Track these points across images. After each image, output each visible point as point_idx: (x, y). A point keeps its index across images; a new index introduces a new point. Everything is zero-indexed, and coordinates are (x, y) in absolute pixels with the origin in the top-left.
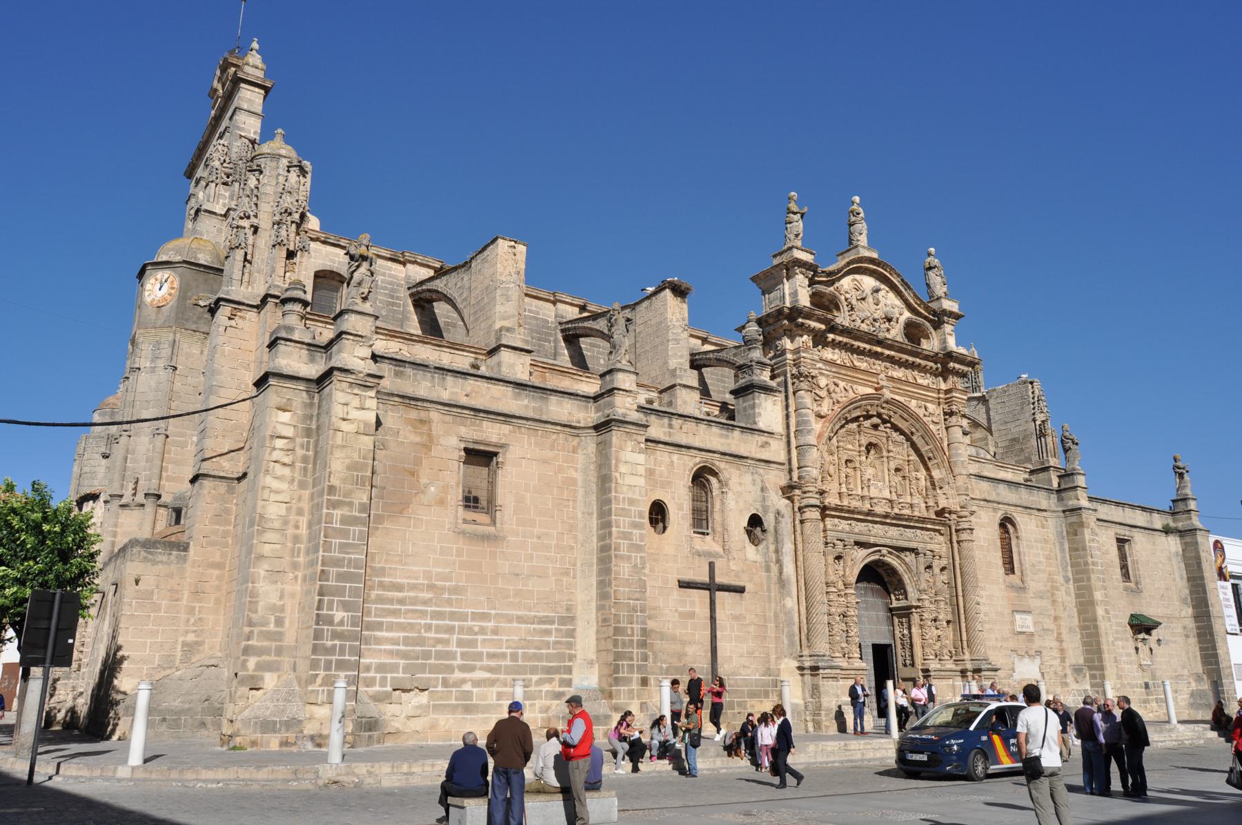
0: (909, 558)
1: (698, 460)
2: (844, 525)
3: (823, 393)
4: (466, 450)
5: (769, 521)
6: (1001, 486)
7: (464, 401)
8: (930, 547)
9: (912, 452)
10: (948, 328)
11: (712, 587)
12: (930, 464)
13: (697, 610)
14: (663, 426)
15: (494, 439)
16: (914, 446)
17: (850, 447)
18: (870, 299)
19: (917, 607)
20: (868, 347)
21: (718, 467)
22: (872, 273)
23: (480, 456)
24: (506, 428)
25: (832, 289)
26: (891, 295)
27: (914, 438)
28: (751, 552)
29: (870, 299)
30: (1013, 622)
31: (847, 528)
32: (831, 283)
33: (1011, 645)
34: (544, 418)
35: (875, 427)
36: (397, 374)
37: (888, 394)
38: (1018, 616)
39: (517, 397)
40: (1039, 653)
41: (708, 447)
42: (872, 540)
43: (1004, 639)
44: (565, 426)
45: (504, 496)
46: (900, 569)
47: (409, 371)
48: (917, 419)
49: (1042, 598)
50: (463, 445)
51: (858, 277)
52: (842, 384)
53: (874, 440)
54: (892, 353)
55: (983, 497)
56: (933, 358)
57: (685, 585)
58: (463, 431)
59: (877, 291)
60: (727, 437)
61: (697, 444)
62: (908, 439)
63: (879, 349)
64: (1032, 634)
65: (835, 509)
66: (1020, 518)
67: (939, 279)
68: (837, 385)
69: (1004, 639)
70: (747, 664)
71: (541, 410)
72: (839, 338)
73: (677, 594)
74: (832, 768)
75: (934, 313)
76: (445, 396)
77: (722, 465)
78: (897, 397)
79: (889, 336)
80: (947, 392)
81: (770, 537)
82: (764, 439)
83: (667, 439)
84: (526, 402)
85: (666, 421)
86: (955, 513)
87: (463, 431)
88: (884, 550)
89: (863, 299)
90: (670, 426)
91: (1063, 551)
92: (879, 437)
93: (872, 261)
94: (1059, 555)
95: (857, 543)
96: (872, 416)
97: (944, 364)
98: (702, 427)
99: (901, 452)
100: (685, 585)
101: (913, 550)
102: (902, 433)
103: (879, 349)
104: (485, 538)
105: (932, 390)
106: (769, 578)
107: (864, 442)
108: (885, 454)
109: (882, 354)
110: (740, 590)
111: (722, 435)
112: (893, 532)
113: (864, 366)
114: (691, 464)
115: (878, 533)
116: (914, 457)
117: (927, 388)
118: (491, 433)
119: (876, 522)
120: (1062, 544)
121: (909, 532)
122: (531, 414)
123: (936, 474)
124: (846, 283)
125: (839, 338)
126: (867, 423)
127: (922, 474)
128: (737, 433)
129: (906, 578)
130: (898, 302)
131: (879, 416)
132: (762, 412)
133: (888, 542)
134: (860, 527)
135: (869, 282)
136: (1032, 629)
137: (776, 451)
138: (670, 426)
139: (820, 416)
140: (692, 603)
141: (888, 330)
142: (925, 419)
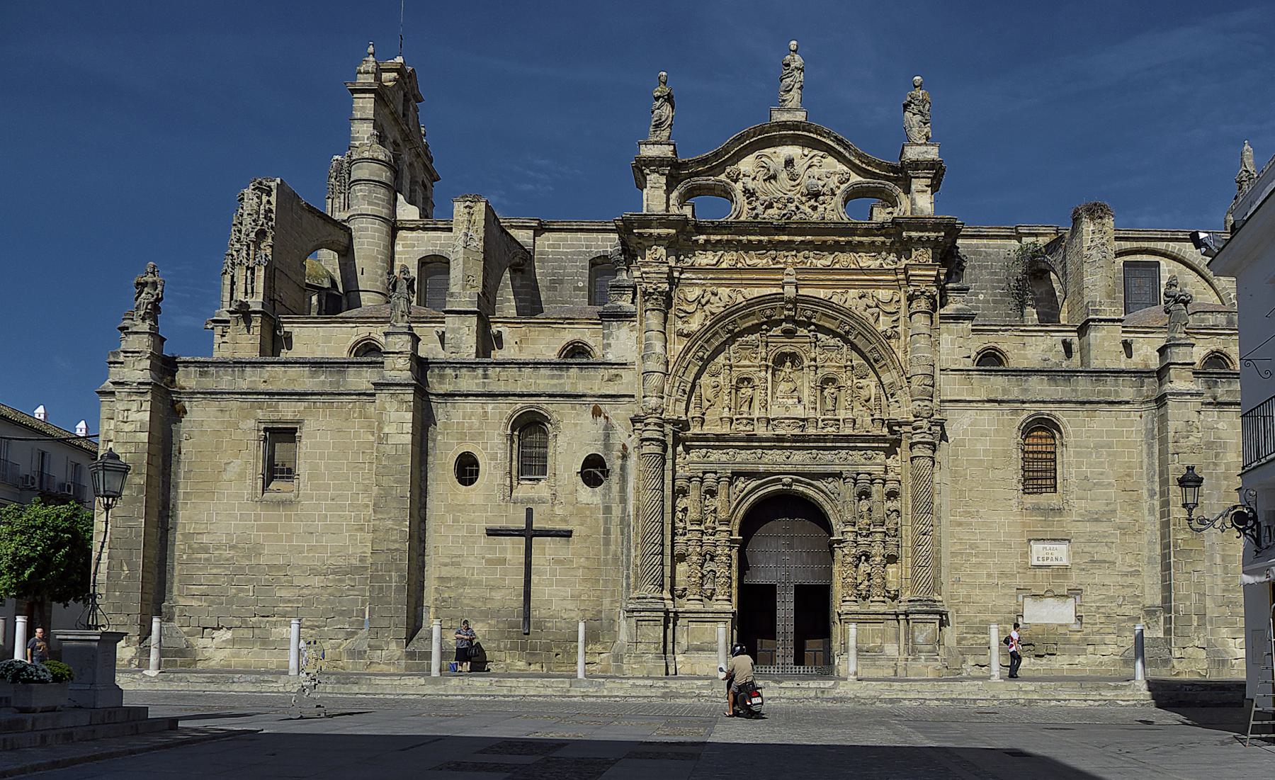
0: (829, 485)
1: (518, 406)
2: (715, 455)
3: (690, 308)
4: (266, 430)
5: (614, 463)
6: (1034, 379)
7: (262, 387)
8: (868, 469)
9: (854, 354)
10: (917, 184)
11: (529, 533)
12: (877, 366)
13: (509, 557)
14: (476, 377)
15: (289, 417)
16: (854, 347)
17: (747, 362)
18: (783, 175)
19: (839, 542)
20: (765, 238)
21: (546, 411)
22: (794, 141)
23: (281, 434)
24: (301, 406)
25: (722, 177)
26: (830, 160)
27: (851, 337)
28: (587, 495)
29: (783, 175)
30: (1026, 555)
31: (724, 458)
32: (721, 168)
33: (1019, 581)
34: (342, 389)
35: (789, 333)
36: (202, 374)
37: (790, 291)
38: (1037, 548)
39: (313, 375)
40: (1075, 592)
41: (532, 390)
42: (762, 468)
43: (1003, 574)
44: (359, 394)
45: (302, 468)
46: (819, 498)
47: (212, 370)
48: (848, 313)
49: (1097, 520)
50: (263, 426)
51: (767, 151)
52: (724, 292)
53: (787, 350)
54: (809, 238)
55: (992, 397)
56: (881, 229)
57: (492, 533)
58: (260, 414)
59: (789, 162)
60: (560, 377)
61: (518, 391)
62: (846, 341)
63: (785, 238)
64: (1066, 568)
65: (692, 440)
66: (1063, 416)
67: (918, 117)
68: (715, 294)
69: (1003, 574)
70: (569, 607)
71: (338, 383)
72: (714, 238)
73: (484, 541)
74: (637, 706)
75: (894, 169)
76: (244, 385)
77: (550, 408)
78: (822, 293)
79: (815, 217)
80: (906, 270)
81: (614, 478)
82: (614, 372)
83: (480, 390)
84: (323, 378)
85: (480, 372)
86: (908, 424)
87: (260, 414)
88: (787, 479)
89: (774, 177)
90: (485, 376)
91: (1150, 455)
92: (802, 343)
93: (784, 125)
94: (1146, 460)
95: (736, 475)
96: (779, 323)
97: (897, 237)
98: (527, 371)
99: (836, 358)
100: (492, 533)
101: (838, 475)
102: (835, 334)
103: (785, 238)
104: (283, 503)
105: (887, 272)
106: (606, 521)
107: (774, 351)
108: (806, 363)
109: (793, 242)
110: (568, 534)
111: (552, 377)
112: (798, 456)
113: (761, 263)
114: (510, 412)
115: (773, 459)
116: (857, 360)
117: (881, 270)
118: (287, 411)
119: (771, 448)
120: (1150, 446)
121: (828, 456)
122: (328, 389)
123: (886, 378)
124: (747, 164)
125: (714, 238)
126: (777, 331)
127: (870, 384)
128: (574, 371)
129: (827, 507)
130: (842, 168)
131: (788, 319)
132: (612, 341)
133: (788, 468)
134: (744, 455)
135: (794, 151)
136: (1065, 562)
137: (628, 382)
138: (485, 376)
139: (680, 334)
140: (505, 549)
141: (814, 208)
142: (867, 314)
